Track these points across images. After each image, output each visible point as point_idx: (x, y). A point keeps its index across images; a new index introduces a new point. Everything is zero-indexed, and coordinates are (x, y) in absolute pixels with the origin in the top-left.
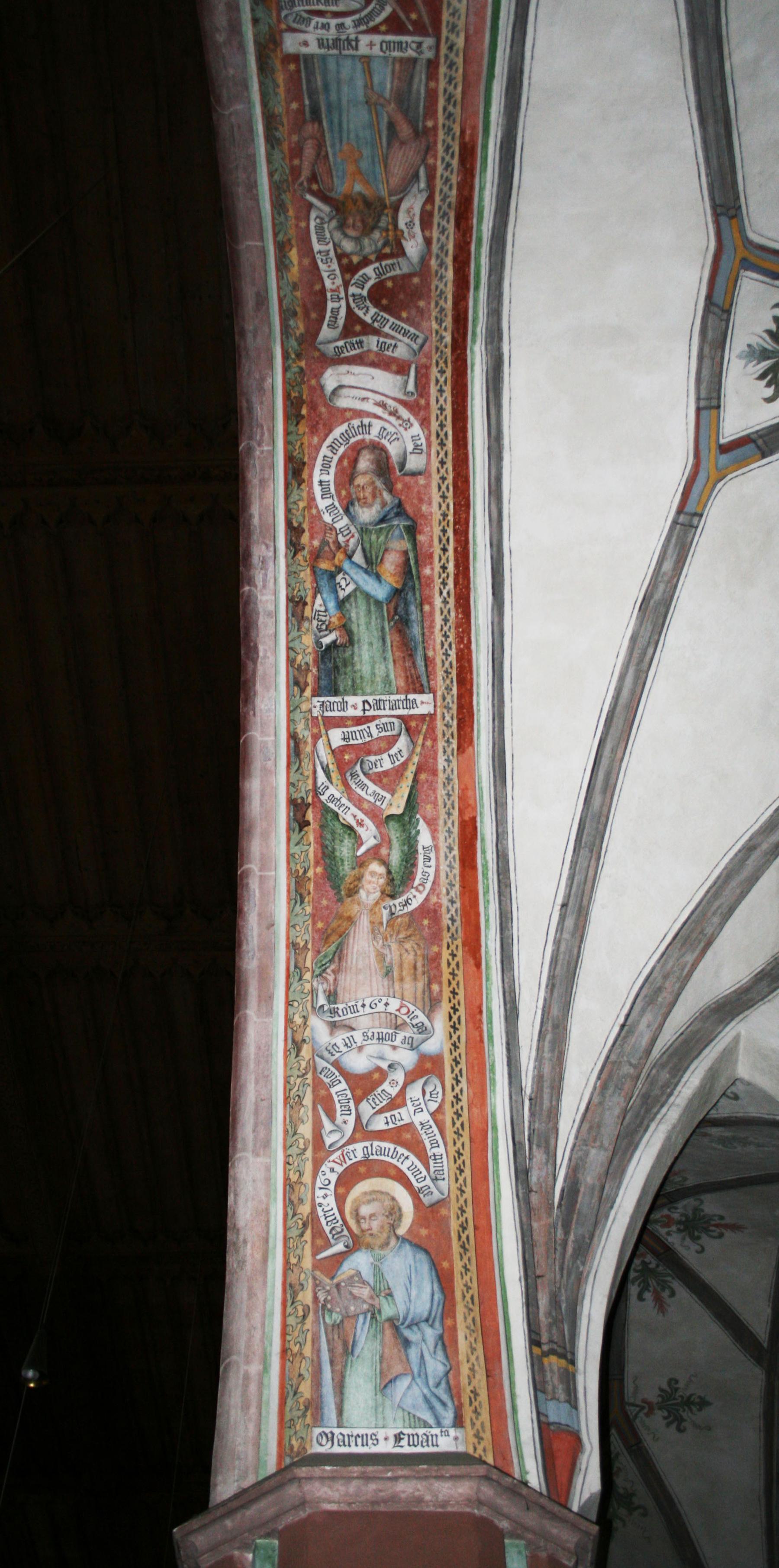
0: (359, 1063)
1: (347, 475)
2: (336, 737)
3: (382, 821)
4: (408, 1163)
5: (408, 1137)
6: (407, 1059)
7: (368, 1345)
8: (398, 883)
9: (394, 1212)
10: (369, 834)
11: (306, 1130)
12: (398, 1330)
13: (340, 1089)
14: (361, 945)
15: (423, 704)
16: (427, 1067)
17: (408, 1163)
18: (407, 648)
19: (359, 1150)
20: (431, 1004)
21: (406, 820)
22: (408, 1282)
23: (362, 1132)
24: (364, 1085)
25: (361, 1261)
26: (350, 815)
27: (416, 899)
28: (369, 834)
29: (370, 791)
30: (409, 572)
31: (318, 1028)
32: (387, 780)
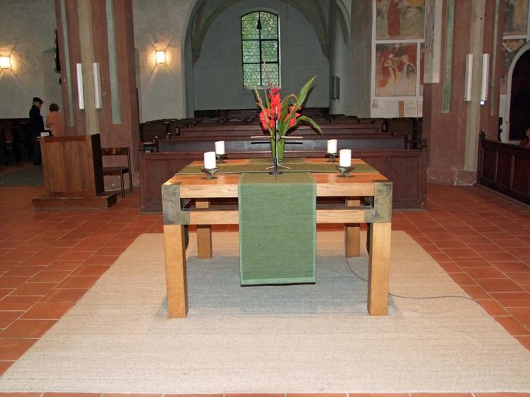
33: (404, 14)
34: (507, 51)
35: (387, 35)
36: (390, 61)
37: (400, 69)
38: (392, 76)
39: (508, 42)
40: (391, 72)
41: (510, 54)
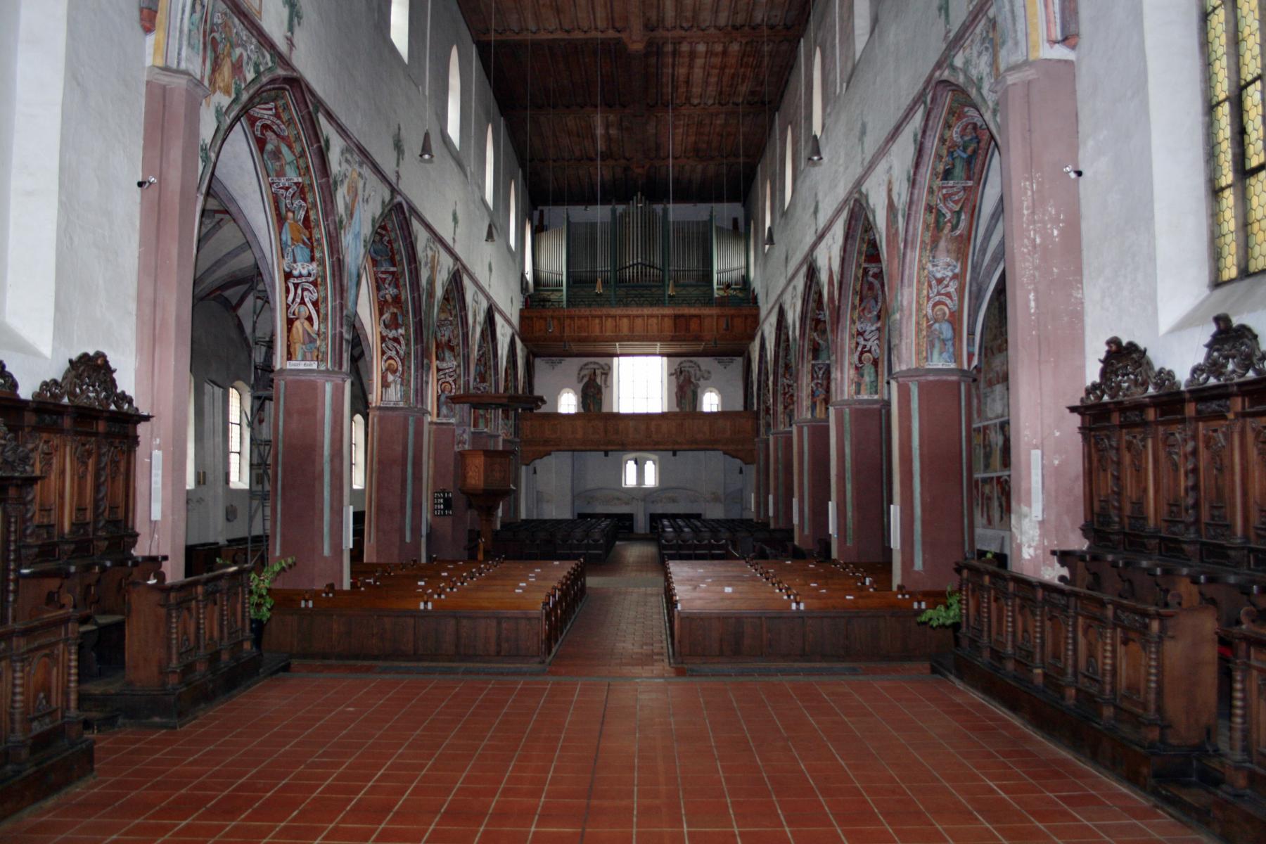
0: (939, 275)
1: (964, 129)
2: (944, 191)
3: (953, 212)
4: (948, 301)
5: (948, 295)
6: (950, 274)
7: (937, 344)
8: (954, 228)
9: (944, 314)
10: (948, 216)
11: (925, 292)
12: (944, 342)
13: (934, 282)
14: (942, 244)
15: (970, 183)
16: (955, 277)
17: (948, 301)
18: (969, 169)
19: (937, 298)
20: (957, 260)
21: (959, 213)
22: (947, 331)
23: (939, 294)
24: (940, 281)
25: (937, 326)
26: (944, 211)
27: (958, 232)
28: (948, 216)
29: (951, 204)
30: (975, 152)
31: (929, 266)
32: (956, 202)
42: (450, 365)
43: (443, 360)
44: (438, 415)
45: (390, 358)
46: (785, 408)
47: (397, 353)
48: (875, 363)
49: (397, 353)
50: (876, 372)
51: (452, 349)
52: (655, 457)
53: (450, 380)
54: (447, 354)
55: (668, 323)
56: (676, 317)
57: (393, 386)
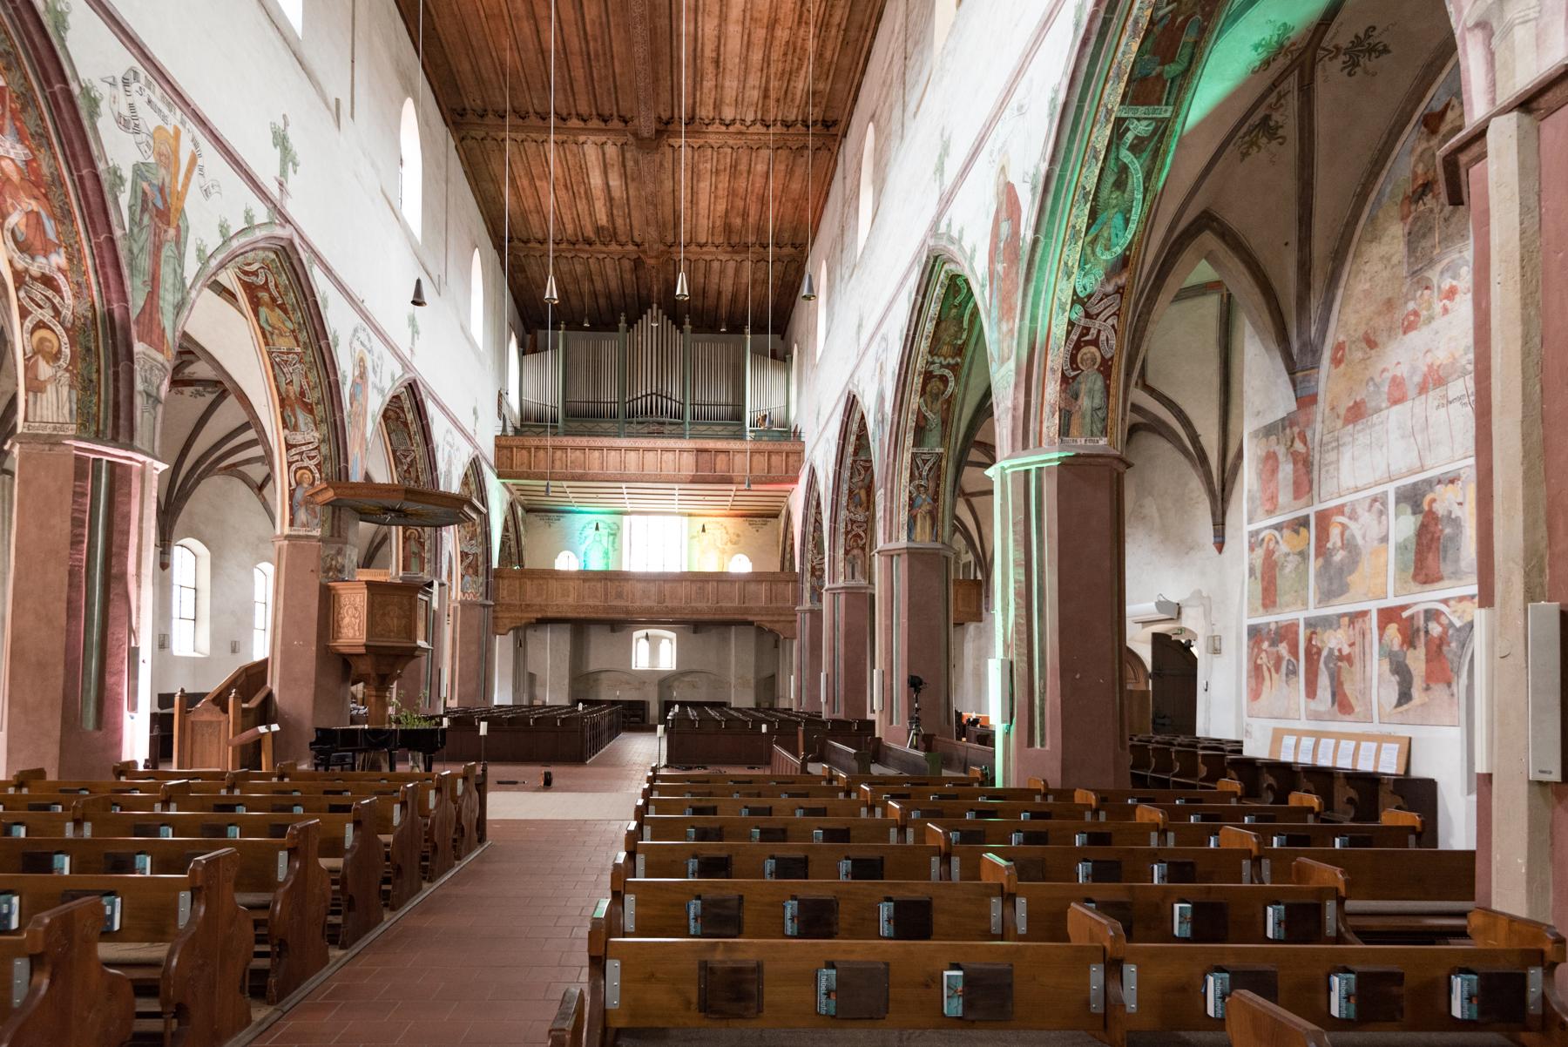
33: (1283, 567)
34: (1451, 624)
35: (1261, 609)
36: (1263, 655)
37: (1277, 670)
38: (1267, 682)
39: (1452, 603)
40: (1266, 674)
41: (1458, 630)
42: (309, 438)
43: (295, 428)
44: (292, 524)
45: (40, 325)
46: (847, 552)
47: (57, 313)
48: (1106, 368)
49: (57, 313)
50: (1107, 388)
51: (309, 409)
52: (673, 635)
53: (312, 464)
54: (302, 418)
55: (688, 460)
56: (699, 451)
57: (50, 388)
